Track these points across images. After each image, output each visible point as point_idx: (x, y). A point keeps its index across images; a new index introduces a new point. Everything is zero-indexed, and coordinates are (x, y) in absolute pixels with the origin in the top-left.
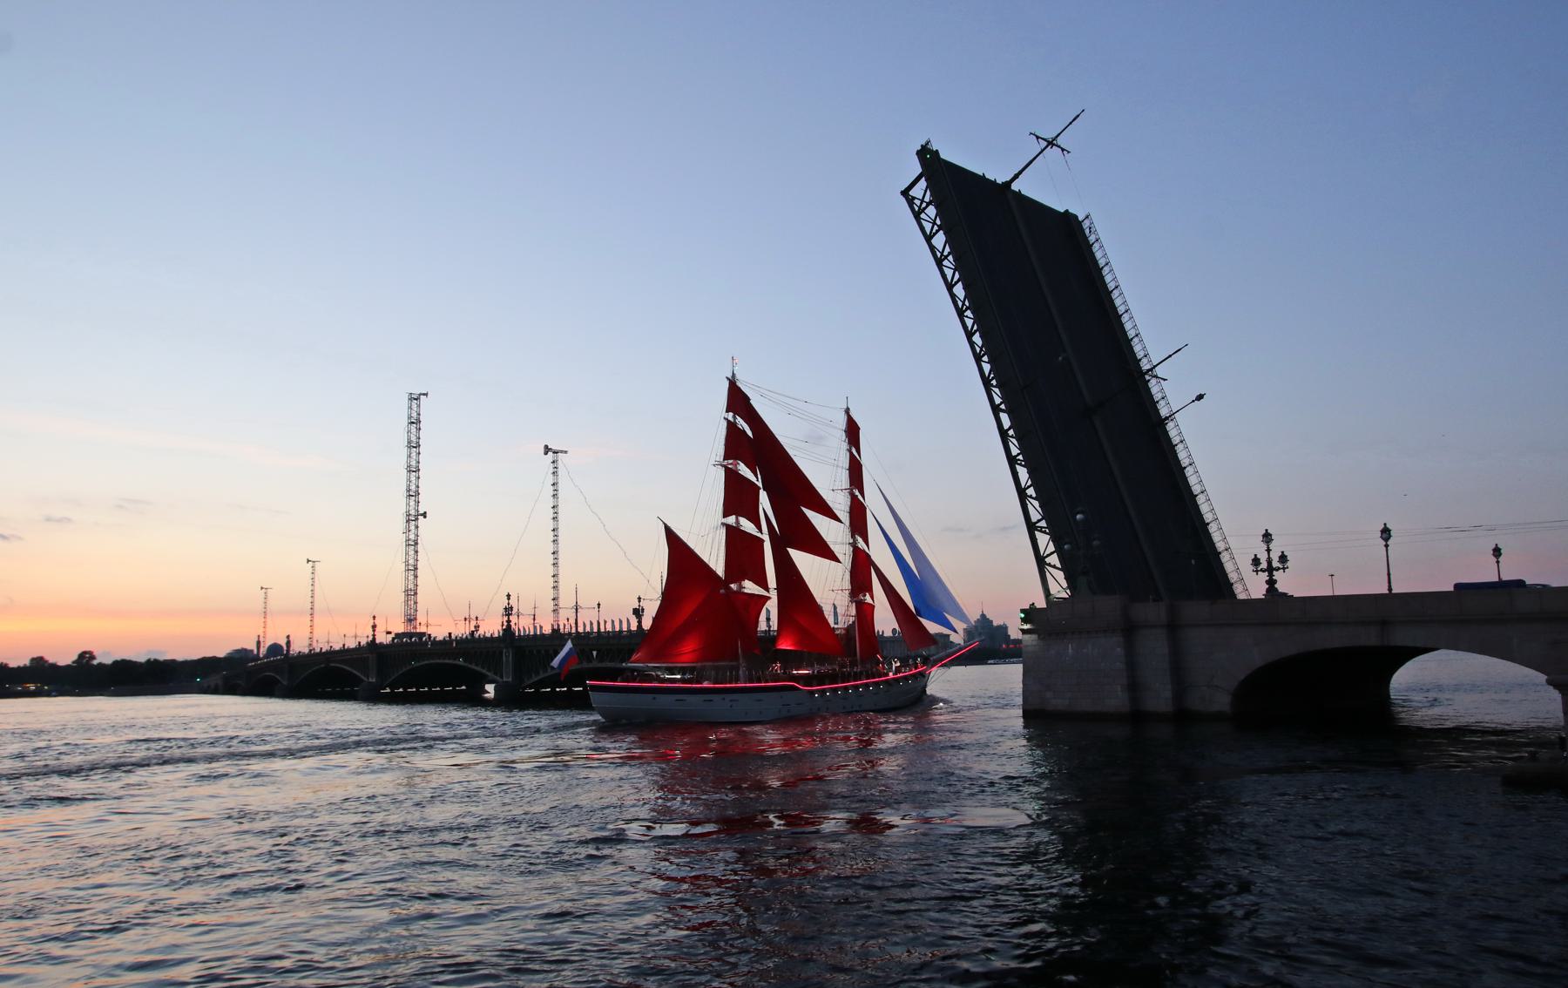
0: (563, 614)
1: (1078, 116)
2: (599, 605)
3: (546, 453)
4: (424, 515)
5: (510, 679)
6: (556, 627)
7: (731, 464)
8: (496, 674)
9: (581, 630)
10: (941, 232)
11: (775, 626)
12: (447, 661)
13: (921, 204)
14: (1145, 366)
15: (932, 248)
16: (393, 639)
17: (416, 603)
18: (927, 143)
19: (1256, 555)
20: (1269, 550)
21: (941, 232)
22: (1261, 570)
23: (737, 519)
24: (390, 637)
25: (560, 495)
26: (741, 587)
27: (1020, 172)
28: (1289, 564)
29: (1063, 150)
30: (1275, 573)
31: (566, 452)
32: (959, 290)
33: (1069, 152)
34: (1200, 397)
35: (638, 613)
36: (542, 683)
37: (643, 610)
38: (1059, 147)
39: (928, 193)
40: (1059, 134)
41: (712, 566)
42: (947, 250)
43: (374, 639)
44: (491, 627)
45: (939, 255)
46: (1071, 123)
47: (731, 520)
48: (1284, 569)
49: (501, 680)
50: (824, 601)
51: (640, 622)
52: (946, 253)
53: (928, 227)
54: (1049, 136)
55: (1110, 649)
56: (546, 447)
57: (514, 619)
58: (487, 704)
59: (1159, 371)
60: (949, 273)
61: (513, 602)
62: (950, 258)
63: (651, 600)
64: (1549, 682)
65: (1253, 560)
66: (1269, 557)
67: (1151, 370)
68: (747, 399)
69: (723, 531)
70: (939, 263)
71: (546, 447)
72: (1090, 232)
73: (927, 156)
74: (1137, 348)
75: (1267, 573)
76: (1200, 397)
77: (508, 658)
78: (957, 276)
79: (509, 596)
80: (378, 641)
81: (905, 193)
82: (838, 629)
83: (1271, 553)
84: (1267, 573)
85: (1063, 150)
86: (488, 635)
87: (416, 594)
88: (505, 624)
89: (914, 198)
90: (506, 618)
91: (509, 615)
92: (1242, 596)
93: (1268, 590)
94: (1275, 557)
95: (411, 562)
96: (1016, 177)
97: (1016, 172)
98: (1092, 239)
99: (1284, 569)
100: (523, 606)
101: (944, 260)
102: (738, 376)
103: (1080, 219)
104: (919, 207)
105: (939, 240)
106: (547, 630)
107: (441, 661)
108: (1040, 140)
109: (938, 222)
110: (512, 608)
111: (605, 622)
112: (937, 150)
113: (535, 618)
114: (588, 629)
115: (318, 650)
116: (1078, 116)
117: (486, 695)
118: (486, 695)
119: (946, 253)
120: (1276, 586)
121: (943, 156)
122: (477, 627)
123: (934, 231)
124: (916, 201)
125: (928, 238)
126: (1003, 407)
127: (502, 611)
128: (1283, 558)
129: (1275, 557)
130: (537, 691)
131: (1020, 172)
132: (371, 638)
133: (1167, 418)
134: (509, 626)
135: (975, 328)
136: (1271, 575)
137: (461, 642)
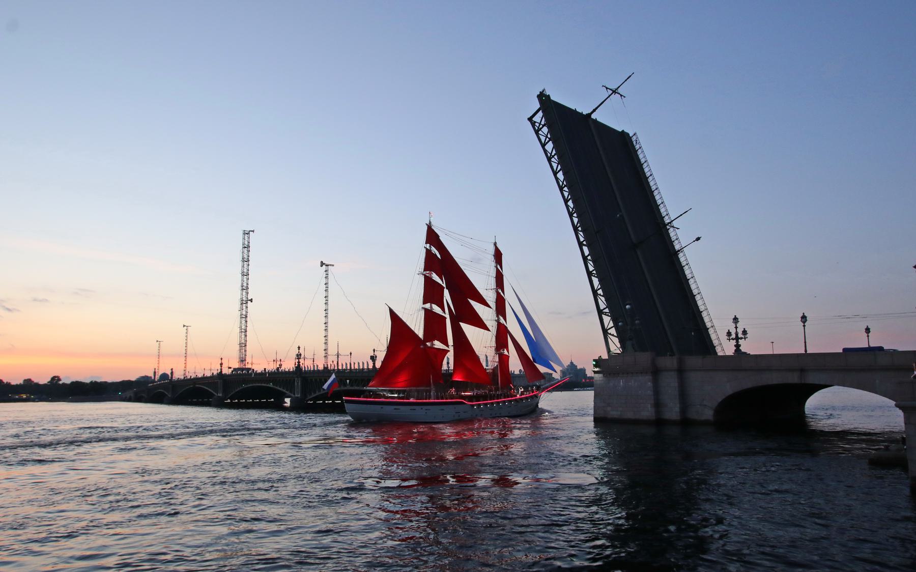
0: (330, 359)
1: (630, 76)
2: (351, 353)
3: (322, 266)
4: (251, 300)
5: (299, 396)
6: (326, 366)
7: (428, 274)
8: (291, 392)
9: (340, 368)
10: (551, 142)
11: (452, 367)
12: (263, 385)
13: (539, 126)
14: (667, 220)
15: (545, 151)
16: (232, 371)
17: (245, 351)
18: (543, 91)
19: (729, 330)
20: (736, 328)
21: (551, 142)
22: (732, 339)
23: (431, 305)
24: (230, 370)
25: (329, 290)
26: (433, 344)
27: (597, 108)
28: (748, 336)
29: (621, 96)
30: (740, 340)
31: (333, 265)
32: (560, 176)
33: (625, 97)
34: (698, 239)
35: (373, 358)
36: (317, 398)
37: (376, 357)
38: (619, 94)
39: (543, 119)
40: (619, 87)
41: (416, 332)
42: (554, 152)
43: (221, 371)
44: (289, 365)
45: (549, 155)
46: (626, 80)
47: (428, 306)
48: (745, 338)
49: (293, 395)
50: (480, 353)
51: (374, 364)
52: (553, 154)
53: (543, 139)
54: (614, 88)
55: (645, 383)
56: (322, 262)
57: (302, 361)
58: (285, 409)
59: (675, 224)
60: (555, 165)
61: (301, 351)
62: (556, 157)
63: (381, 351)
64: (896, 406)
65: (727, 333)
66: (737, 332)
67: (670, 223)
68: (437, 236)
69: (423, 312)
70: (549, 160)
71: (322, 262)
72: (636, 143)
73: (543, 98)
74: (662, 210)
75: (735, 341)
76: (698, 239)
77: (298, 383)
78: (559, 167)
79: (299, 348)
80: (223, 373)
81: (530, 119)
82: (488, 369)
83: (738, 329)
84: (735, 341)
85: (621, 96)
86: (287, 370)
87: (246, 346)
88: (297, 364)
89: (535, 122)
90: (297, 361)
91: (299, 359)
92: (720, 354)
93: (735, 351)
94: (740, 331)
95: (243, 327)
96: (594, 110)
97: (594, 108)
98: (637, 147)
99: (745, 338)
100: (307, 353)
101: (552, 158)
102: (432, 223)
103: (631, 135)
104: (538, 128)
105: (550, 146)
106: (321, 367)
107: (260, 385)
108: (608, 90)
109: (549, 136)
110: (301, 354)
111: (354, 363)
112: (549, 95)
113: (315, 361)
114: (344, 367)
115: (189, 377)
116: (630, 76)
117: (285, 405)
118: (285, 405)
119: (553, 154)
120: (740, 348)
121: (552, 98)
122: (281, 365)
123: (547, 141)
124: (536, 124)
125: (543, 145)
126: (585, 243)
127: (295, 356)
128: (745, 332)
129: (740, 331)
130: (315, 402)
131: (597, 108)
132: (219, 371)
133: (679, 251)
134: (299, 365)
135: (569, 197)
136: (737, 342)
137: (271, 373)
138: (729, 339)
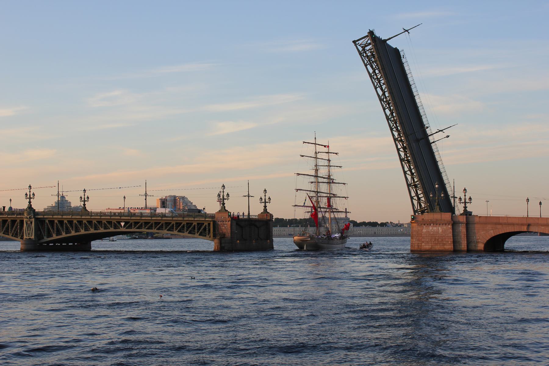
19: (470, 197)
20: (465, 196)
22: (462, 203)
28: (472, 201)
94: (467, 198)
99: (470, 203)
128: (470, 199)
129: (467, 198)
136: (465, 205)
138: (460, 203)
